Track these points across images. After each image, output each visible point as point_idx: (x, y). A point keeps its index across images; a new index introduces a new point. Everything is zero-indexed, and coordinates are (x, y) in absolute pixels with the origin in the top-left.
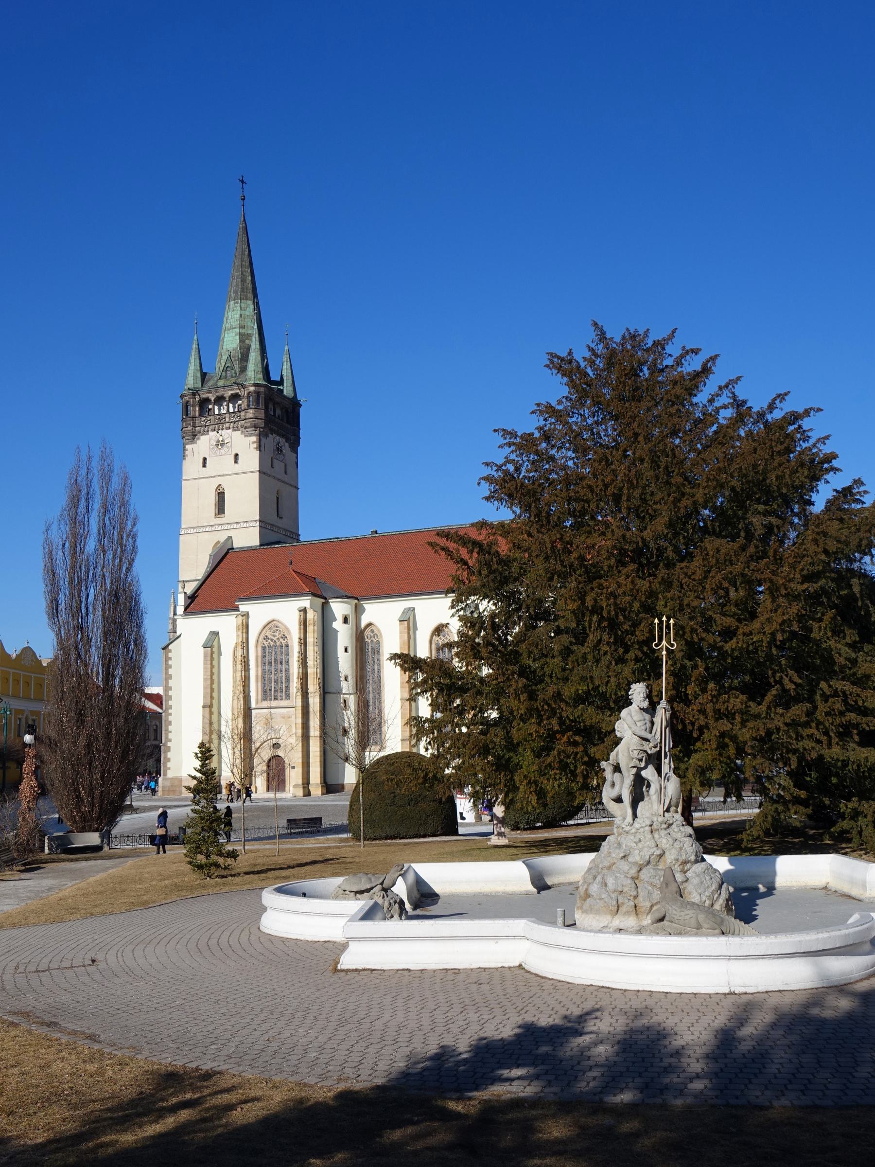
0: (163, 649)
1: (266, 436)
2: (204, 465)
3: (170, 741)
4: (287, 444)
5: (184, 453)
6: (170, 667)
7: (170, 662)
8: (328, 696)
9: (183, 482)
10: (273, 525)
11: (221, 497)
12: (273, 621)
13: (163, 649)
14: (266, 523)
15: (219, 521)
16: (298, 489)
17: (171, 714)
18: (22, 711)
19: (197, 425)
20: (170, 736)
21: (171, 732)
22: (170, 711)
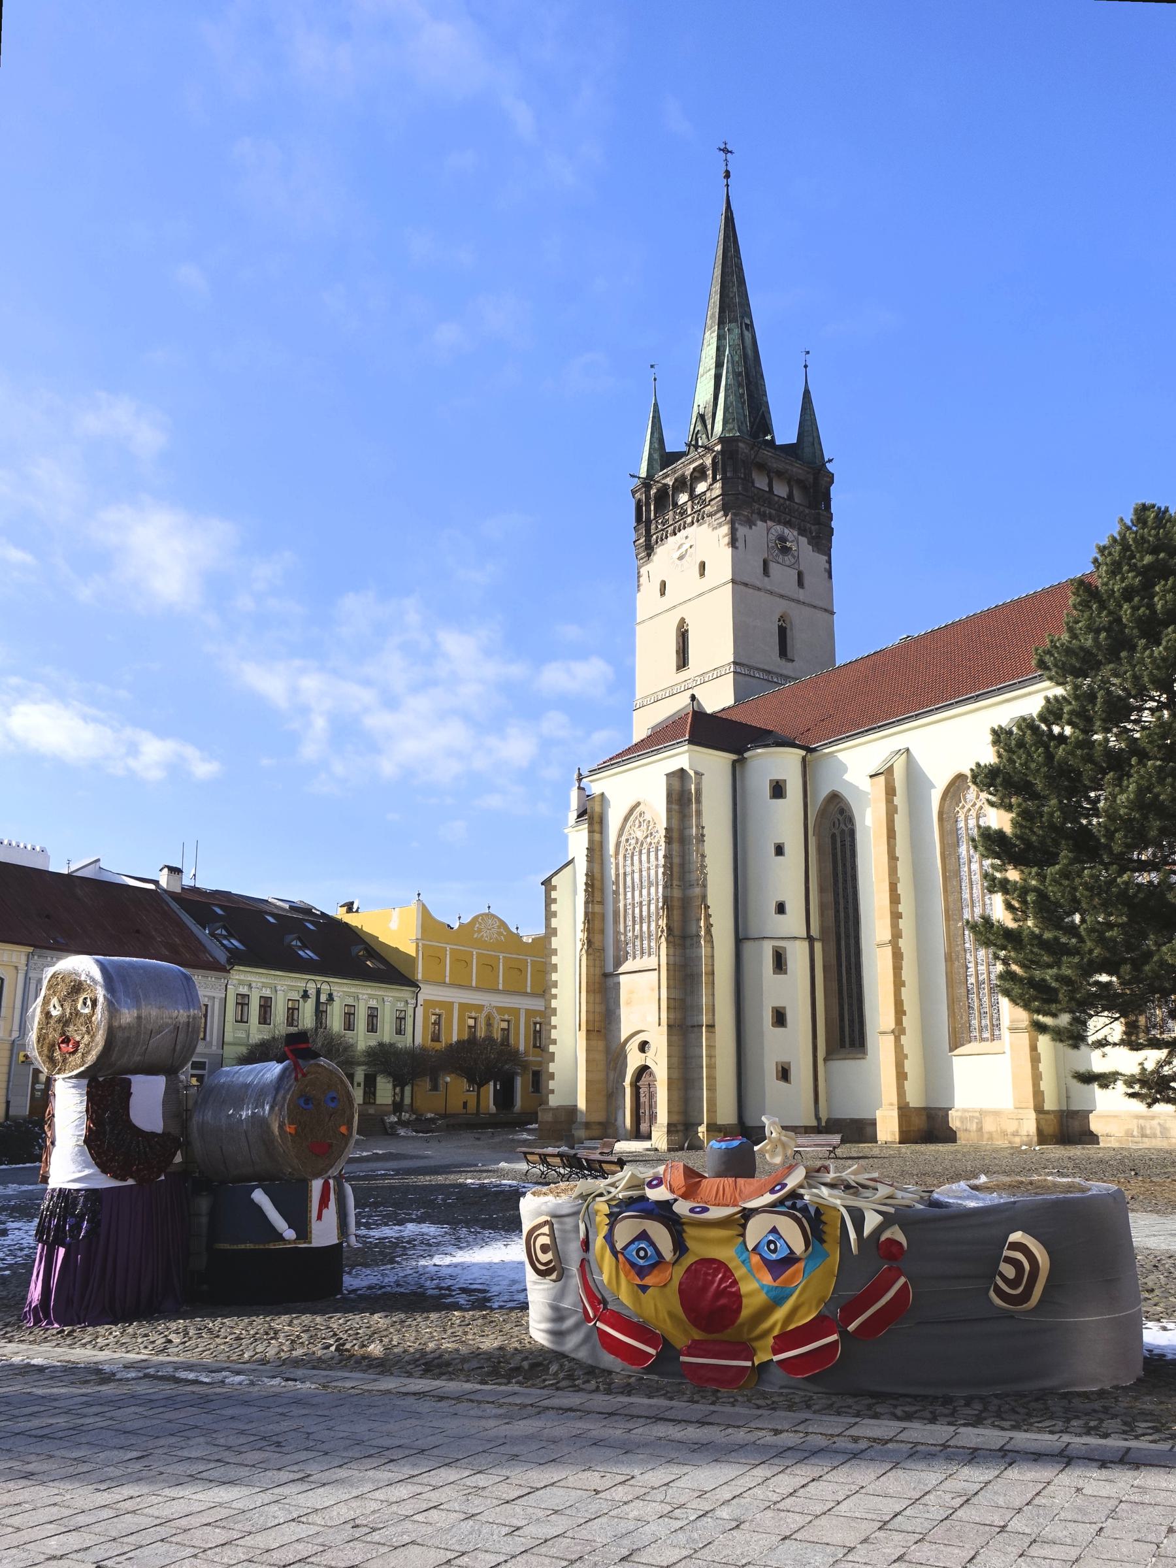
0: (542, 884)
1: (750, 523)
2: (663, 593)
3: (554, 1042)
4: (803, 540)
5: (639, 581)
6: (554, 914)
7: (554, 907)
8: (748, 947)
9: (638, 628)
10: (769, 672)
11: (683, 636)
12: (638, 804)
13: (542, 884)
14: (750, 667)
15: (685, 674)
16: (833, 613)
17: (555, 996)
18: (479, 1008)
19: (653, 531)
20: (554, 1034)
21: (555, 1027)
22: (554, 991)
